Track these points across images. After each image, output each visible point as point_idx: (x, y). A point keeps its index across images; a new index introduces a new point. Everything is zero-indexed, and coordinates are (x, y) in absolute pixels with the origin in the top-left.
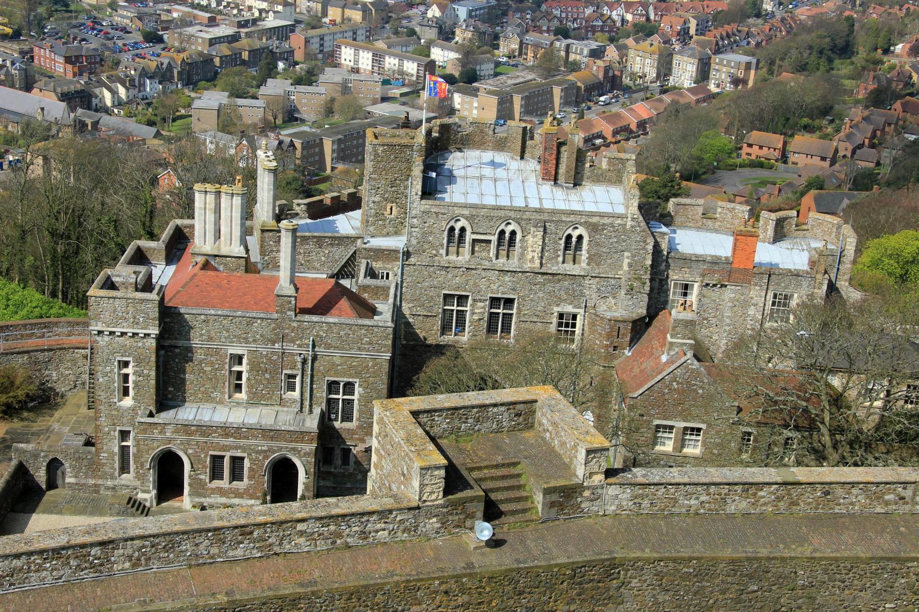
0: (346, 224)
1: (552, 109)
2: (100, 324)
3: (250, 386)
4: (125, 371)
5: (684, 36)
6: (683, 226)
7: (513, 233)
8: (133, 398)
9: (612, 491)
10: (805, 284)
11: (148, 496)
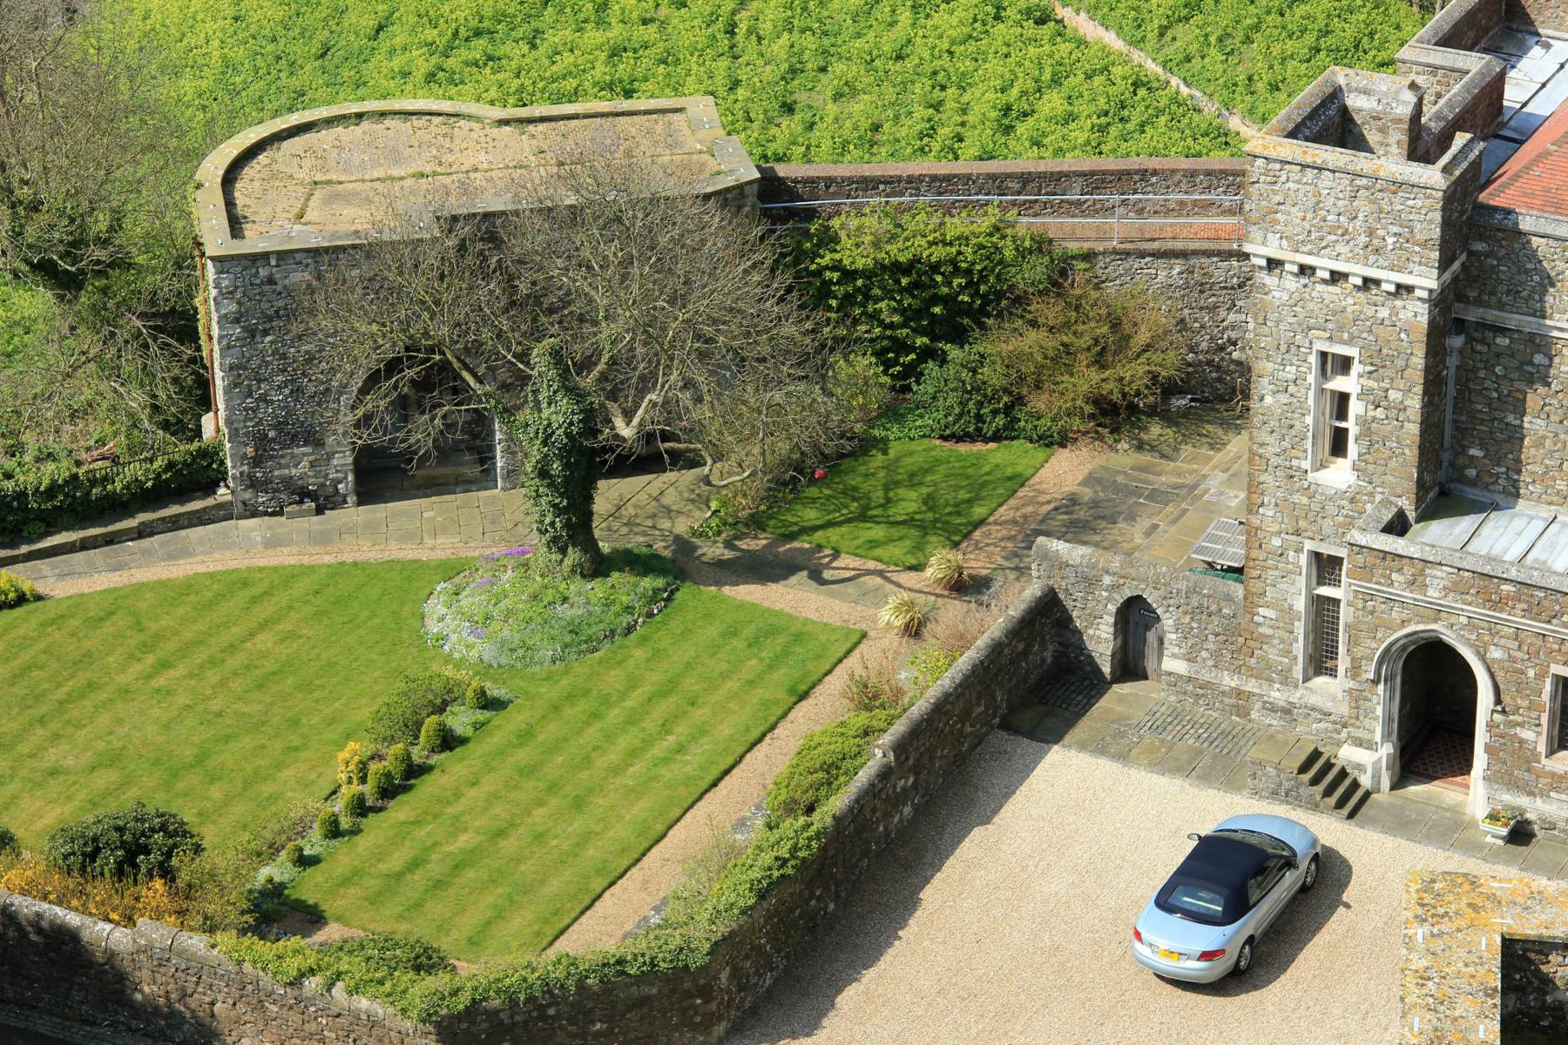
2: (1273, 239)
4: (1339, 383)
8: (1355, 468)
11: (1369, 756)
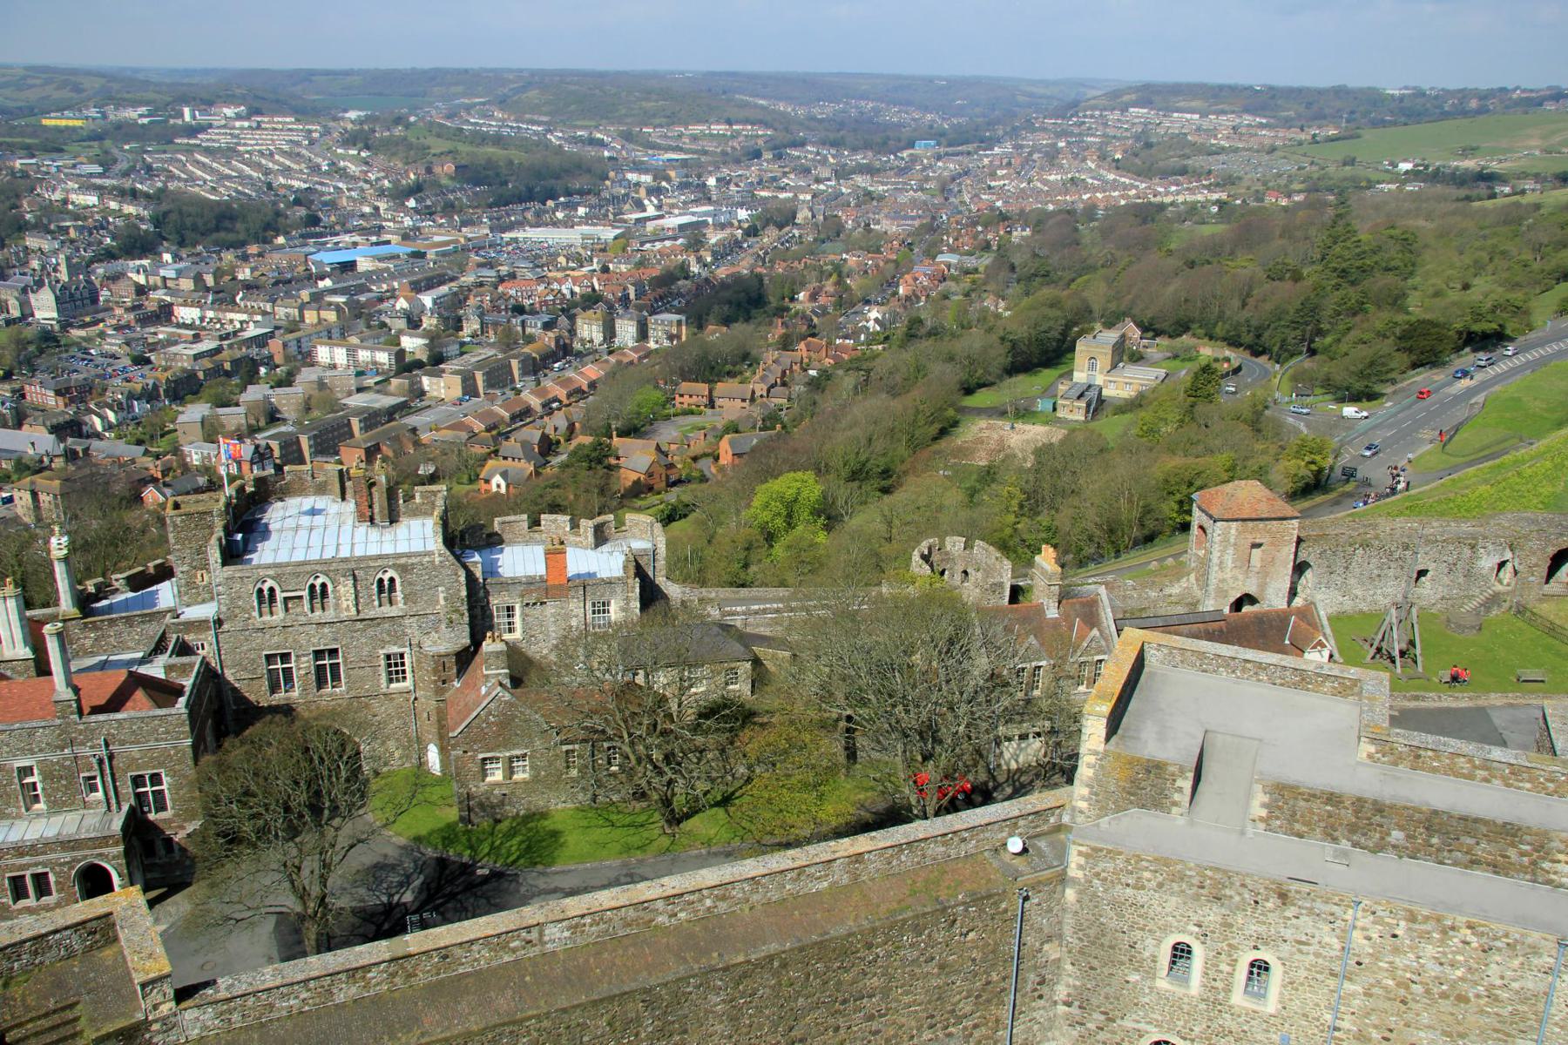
0: (165, 594)
1: (513, 381)
3: (47, 796)
5: (625, 300)
6: (512, 543)
7: (324, 585)
9: (189, 1015)
10: (619, 590)
